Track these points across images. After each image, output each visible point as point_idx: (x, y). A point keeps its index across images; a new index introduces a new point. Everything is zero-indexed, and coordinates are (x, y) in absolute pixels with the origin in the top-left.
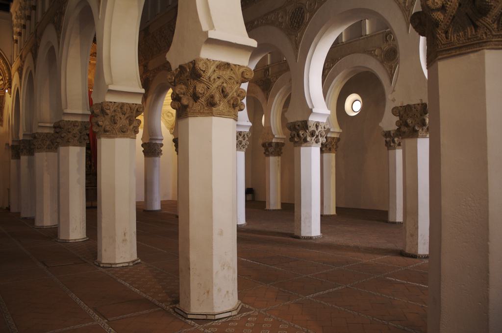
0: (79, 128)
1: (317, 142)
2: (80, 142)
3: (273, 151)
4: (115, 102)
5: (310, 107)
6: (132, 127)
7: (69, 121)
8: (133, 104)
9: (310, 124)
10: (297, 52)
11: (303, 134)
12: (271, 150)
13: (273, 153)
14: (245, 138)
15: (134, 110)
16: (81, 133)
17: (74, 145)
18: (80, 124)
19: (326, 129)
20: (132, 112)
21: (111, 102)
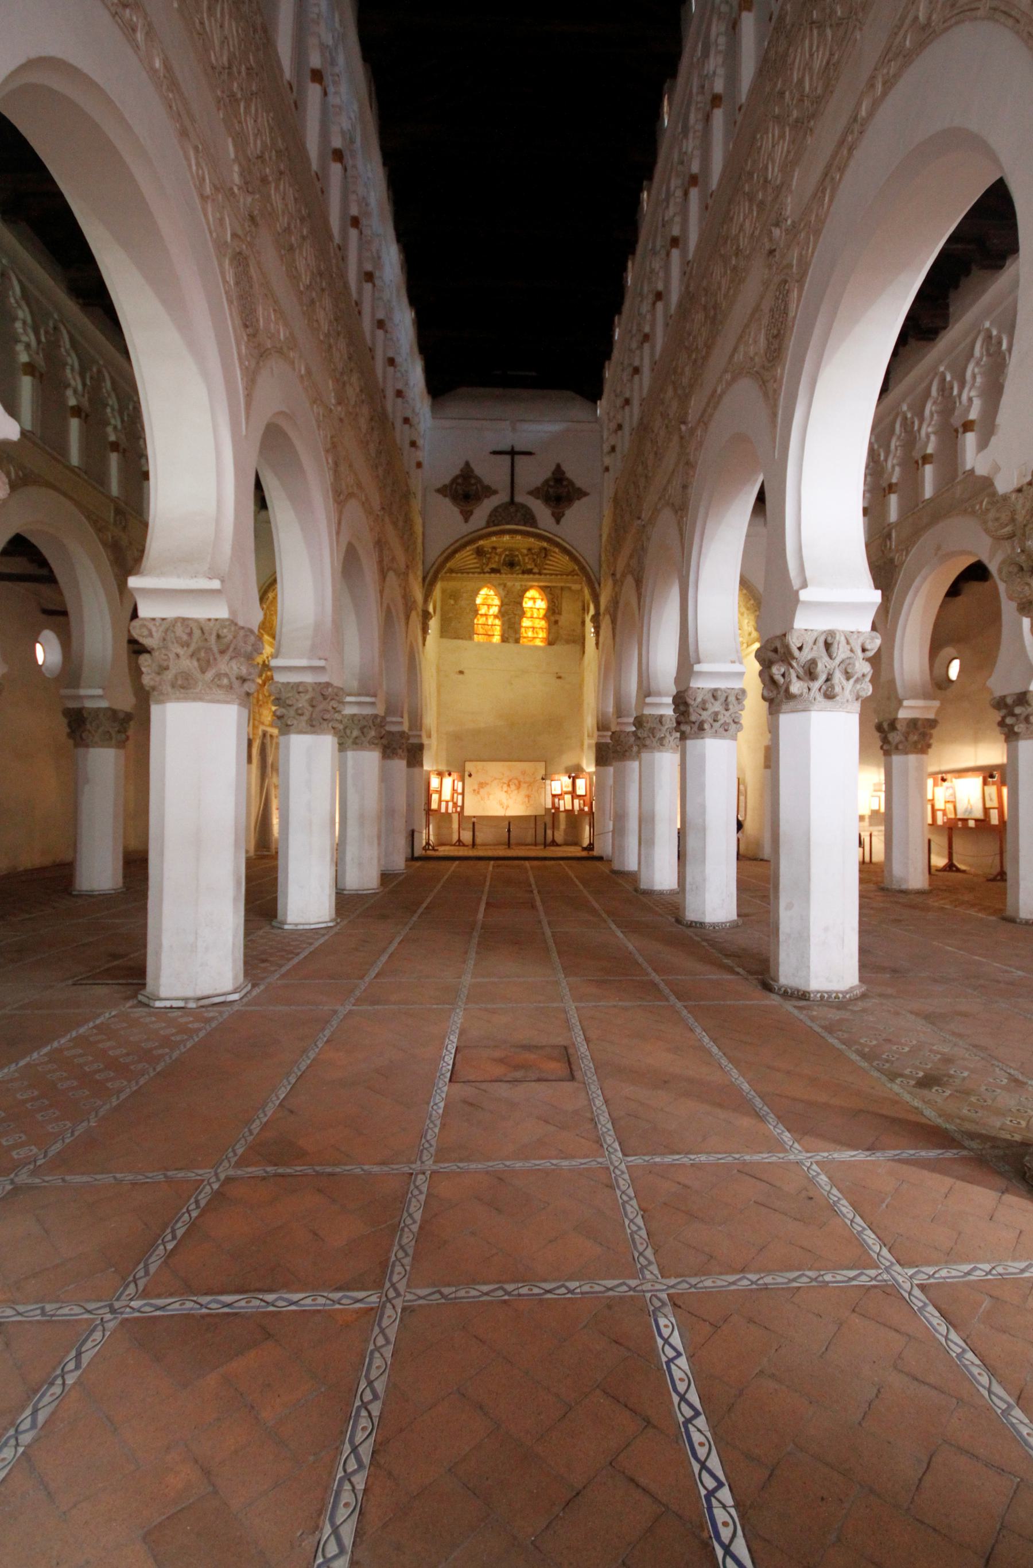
0: (308, 697)
1: (830, 696)
2: (312, 726)
3: (901, 742)
4: (163, 619)
5: (796, 583)
6: (210, 675)
7: (288, 683)
8: (209, 620)
9: (794, 642)
10: (775, 426)
11: (783, 675)
12: (895, 737)
13: (900, 747)
14: (727, 705)
15: (211, 634)
16: (313, 706)
17: (301, 732)
18: (310, 689)
19: (870, 654)
20: (206, 640)
21: (154, 619)
